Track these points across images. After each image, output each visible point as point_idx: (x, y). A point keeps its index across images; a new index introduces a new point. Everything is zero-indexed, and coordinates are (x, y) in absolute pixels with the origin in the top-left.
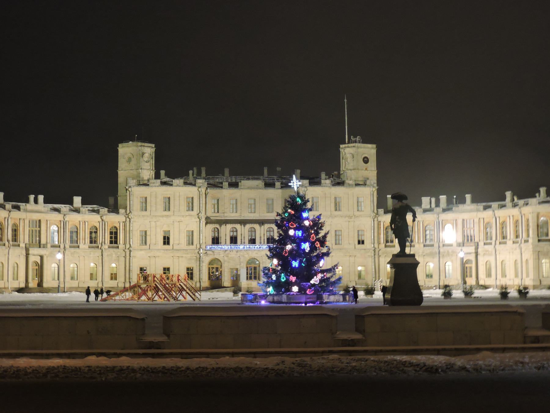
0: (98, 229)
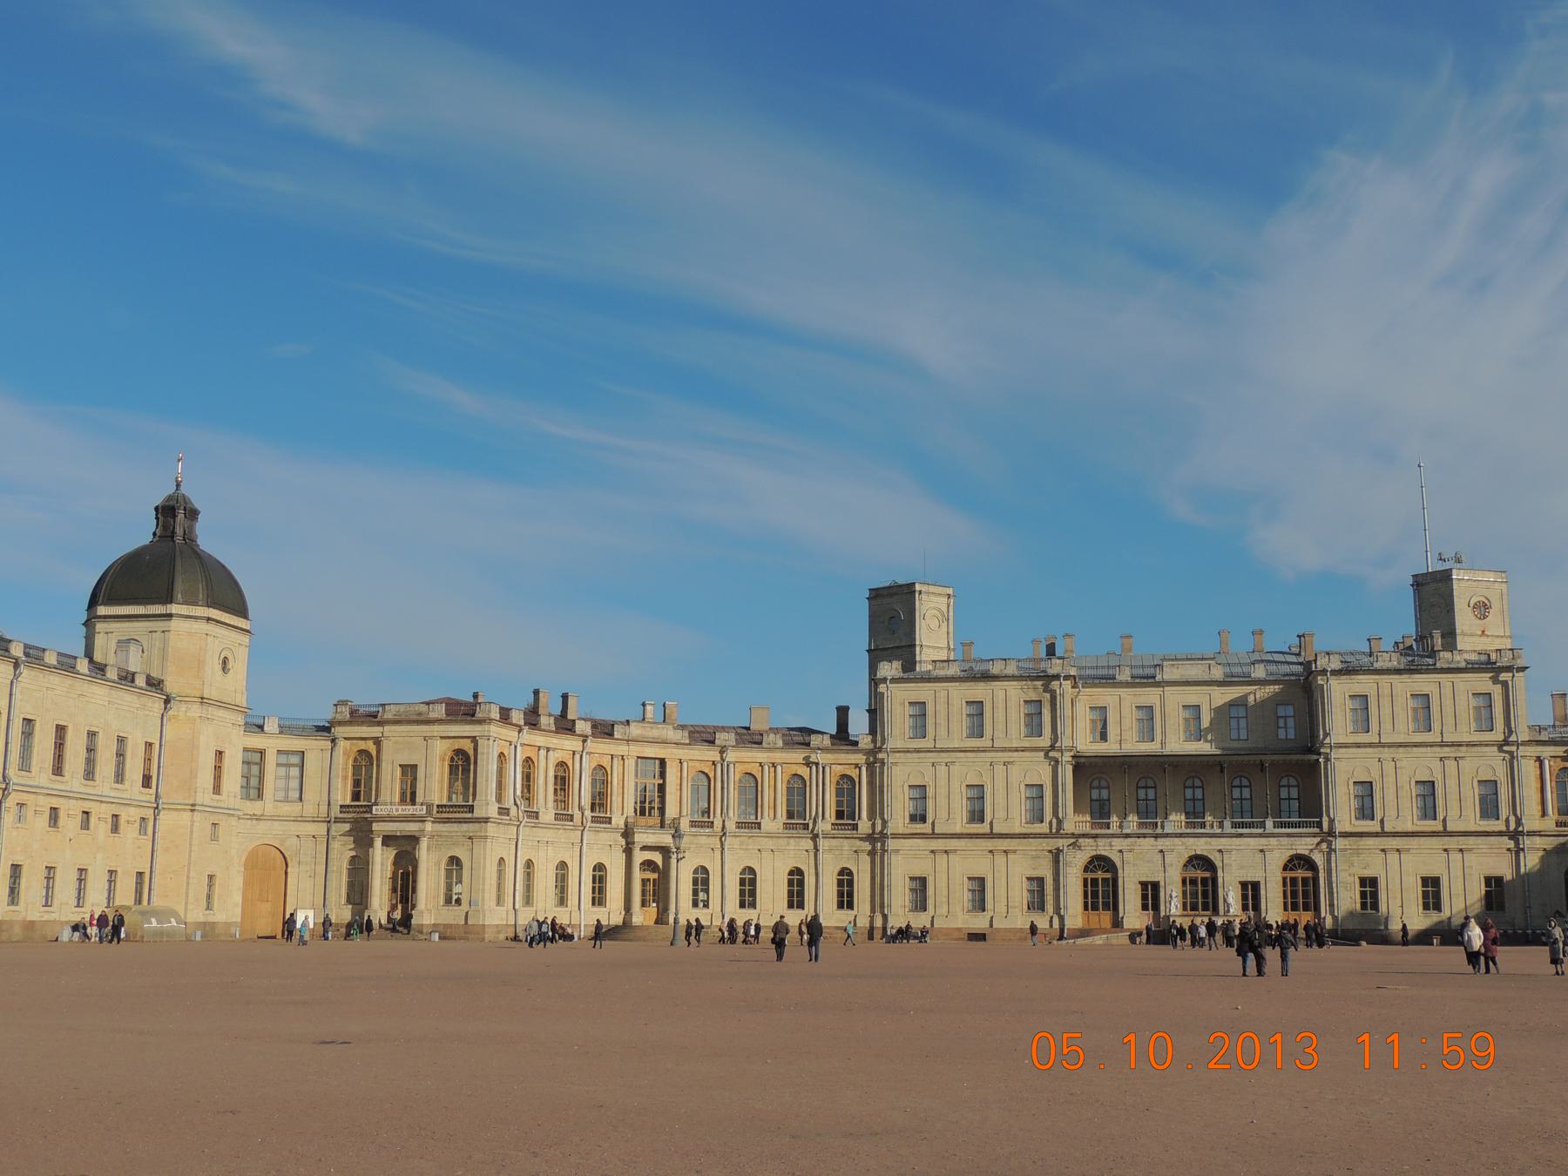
0: (808, 784)
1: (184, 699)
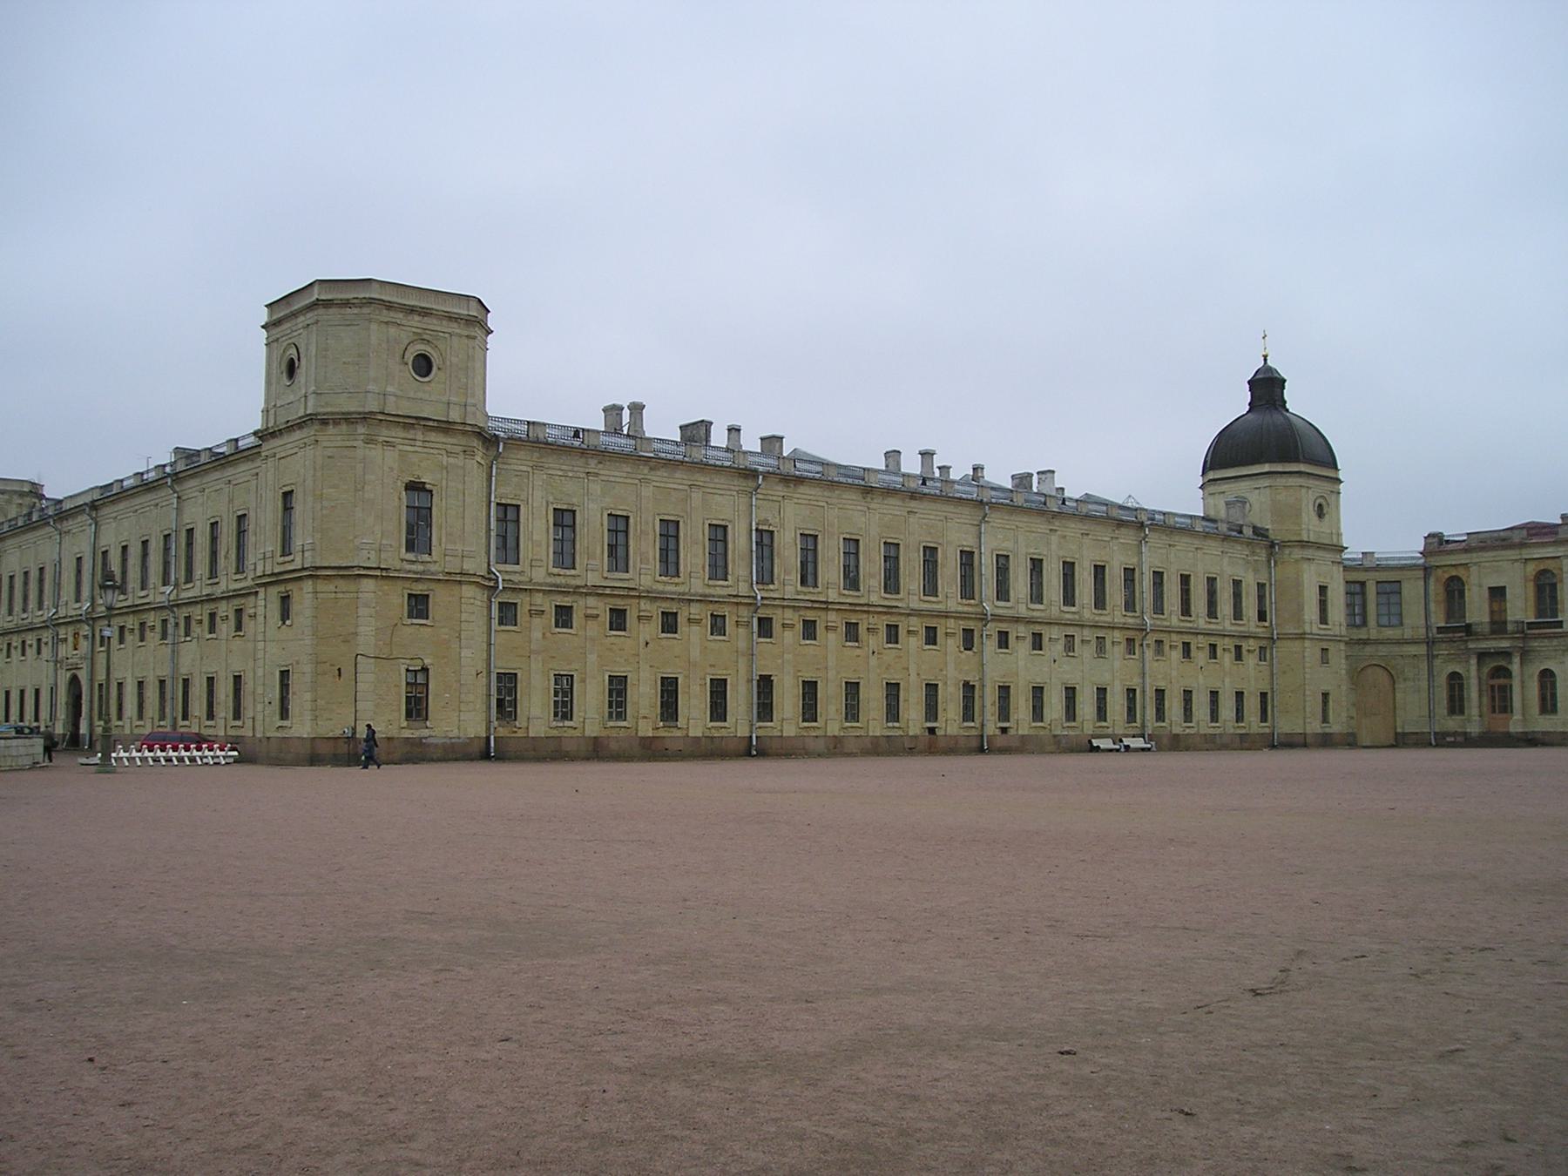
1: (1284, 544)
